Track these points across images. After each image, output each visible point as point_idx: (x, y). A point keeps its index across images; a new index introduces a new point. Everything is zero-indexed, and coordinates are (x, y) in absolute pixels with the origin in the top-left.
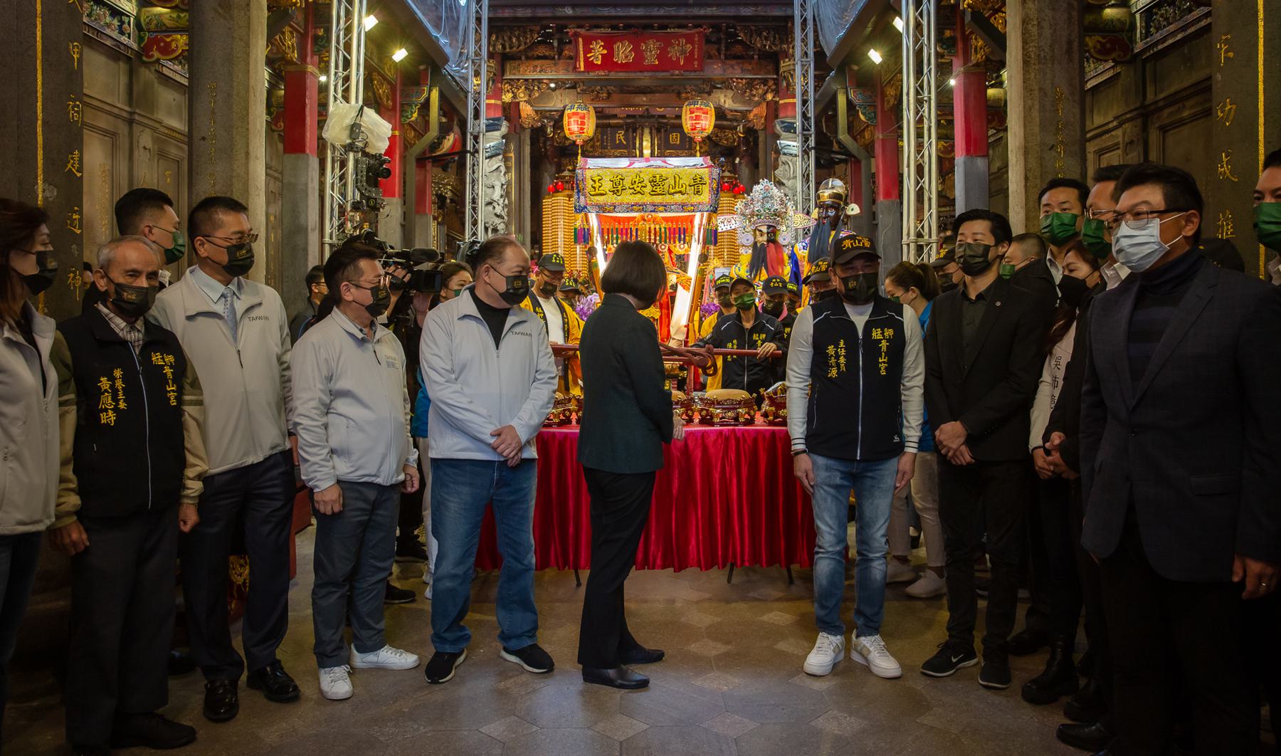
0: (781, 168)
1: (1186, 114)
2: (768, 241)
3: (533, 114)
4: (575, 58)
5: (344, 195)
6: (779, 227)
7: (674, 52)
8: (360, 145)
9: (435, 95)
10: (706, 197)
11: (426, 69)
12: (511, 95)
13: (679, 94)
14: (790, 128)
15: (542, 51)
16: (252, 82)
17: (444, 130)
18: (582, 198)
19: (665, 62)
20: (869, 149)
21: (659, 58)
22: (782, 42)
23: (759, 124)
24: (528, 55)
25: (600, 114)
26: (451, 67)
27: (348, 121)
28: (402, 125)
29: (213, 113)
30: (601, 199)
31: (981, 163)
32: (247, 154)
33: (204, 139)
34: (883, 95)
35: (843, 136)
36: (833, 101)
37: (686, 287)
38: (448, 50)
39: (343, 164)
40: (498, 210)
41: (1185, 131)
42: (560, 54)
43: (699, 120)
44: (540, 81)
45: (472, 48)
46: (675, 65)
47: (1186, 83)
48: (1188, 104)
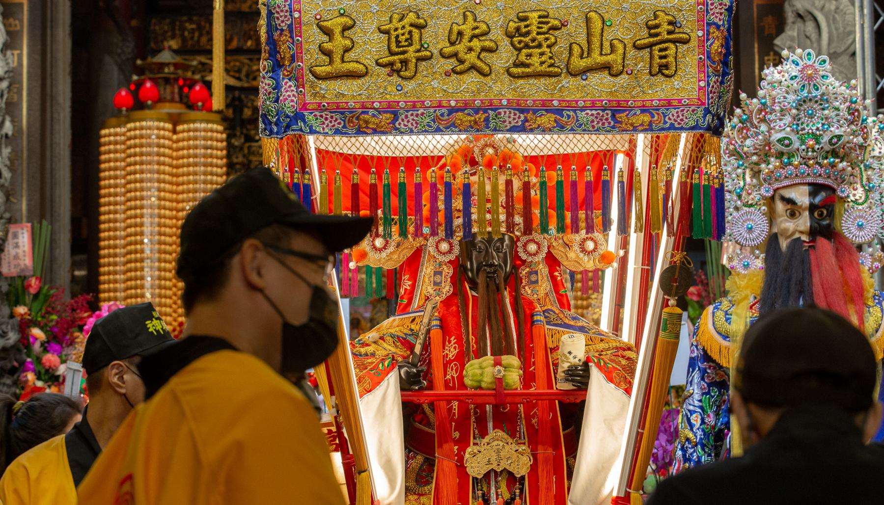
2: (814, 232)
6: (844, 191)
18: (289, 89)
30: (349, 91)
37: (621, 377)
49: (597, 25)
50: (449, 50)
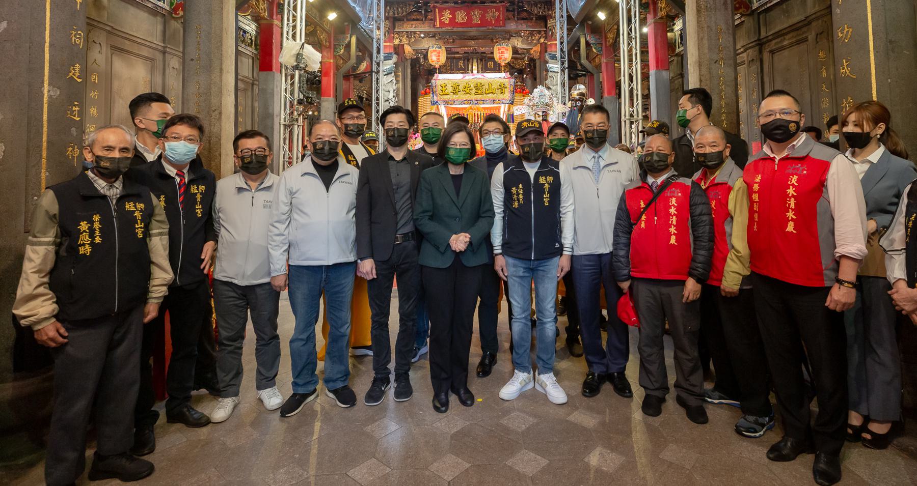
0: (549, 80)
1: (786, 43)
4: (434, 20)
5: (292, 94)
7: (489, 16)
8: (303, 66)
9: (354, 39)
10: (507, 95)
13: (492, 40)
14: (554, 57)
15: (415, 16)
16: (225, 25)
17: (360, 60)
19: (484, 22)
20: (598, 67)
22: (549, 10)
23: (536, 56)
24: (408, 18)
25: (449, 51)
26: (363, 24)
27: (295, 52)
28: (335, 57)
29: (199, 44)
31: (665, 74)
32: (221, 69)
33: (192, 60)
34: (606, 38)
35: (584, 61)
36: (578, 42)
38: (361, 14)
39: (293, 77)
41: (786, 53)
43: (503, 53)
44: (415, 33)
45: (375, 14)
46: (490, 23)
47: (786, 25)
48: (787, 37)
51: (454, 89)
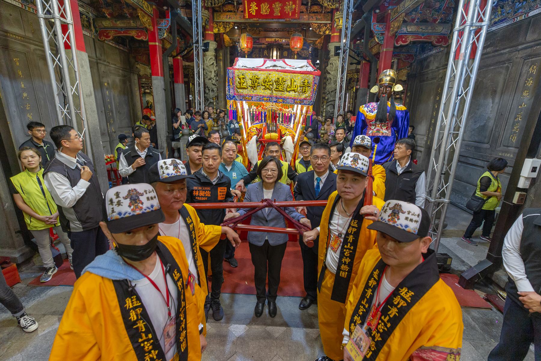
0: (329, 66)
3: (229, 40)
4: (244, 11)
11: (167, 9)
12: (217, 29)
15: (230, 7)
19: (283, 14)
21: (280, 12)
23: (319, 46)
30: (245, 92)
40: (214, 82)
42: (238, 10)
44: (229, 23)
49: (293, 81)
50: (263, 84)
51: (253, 82)
